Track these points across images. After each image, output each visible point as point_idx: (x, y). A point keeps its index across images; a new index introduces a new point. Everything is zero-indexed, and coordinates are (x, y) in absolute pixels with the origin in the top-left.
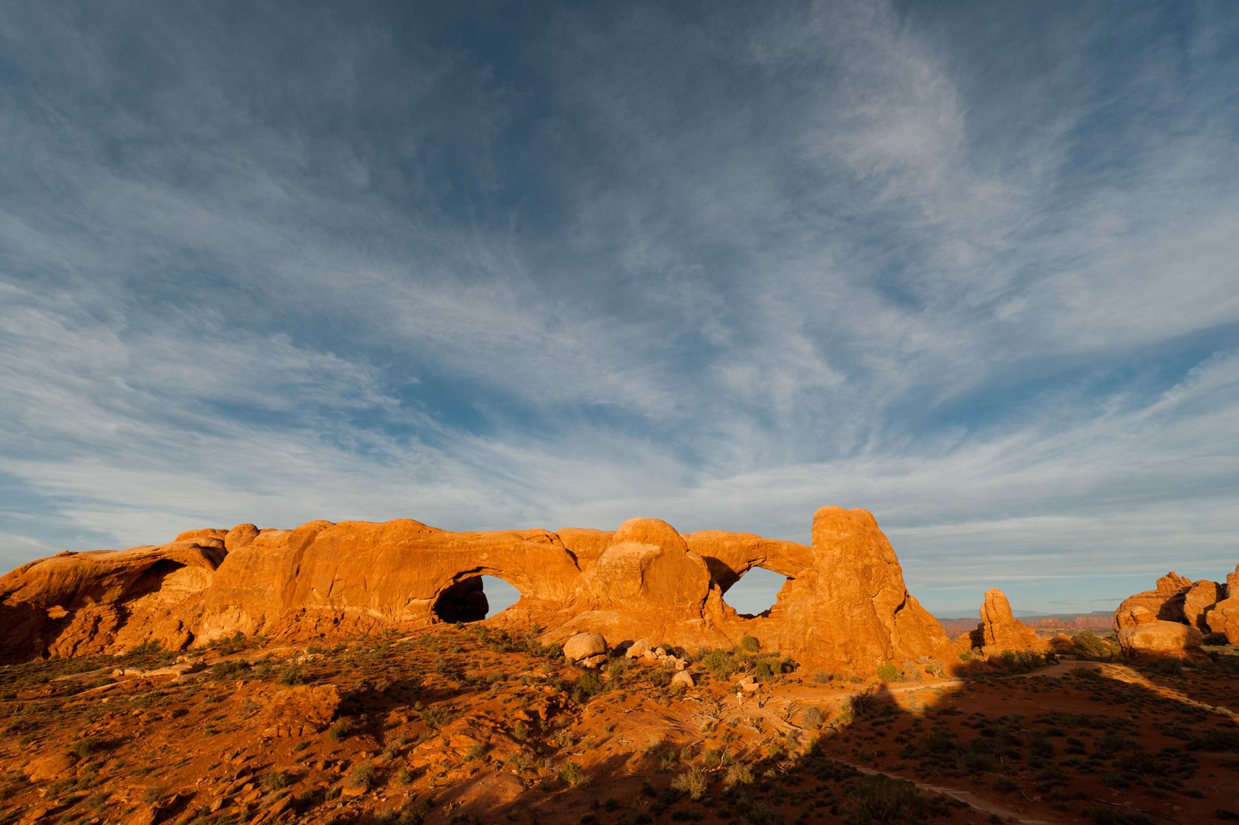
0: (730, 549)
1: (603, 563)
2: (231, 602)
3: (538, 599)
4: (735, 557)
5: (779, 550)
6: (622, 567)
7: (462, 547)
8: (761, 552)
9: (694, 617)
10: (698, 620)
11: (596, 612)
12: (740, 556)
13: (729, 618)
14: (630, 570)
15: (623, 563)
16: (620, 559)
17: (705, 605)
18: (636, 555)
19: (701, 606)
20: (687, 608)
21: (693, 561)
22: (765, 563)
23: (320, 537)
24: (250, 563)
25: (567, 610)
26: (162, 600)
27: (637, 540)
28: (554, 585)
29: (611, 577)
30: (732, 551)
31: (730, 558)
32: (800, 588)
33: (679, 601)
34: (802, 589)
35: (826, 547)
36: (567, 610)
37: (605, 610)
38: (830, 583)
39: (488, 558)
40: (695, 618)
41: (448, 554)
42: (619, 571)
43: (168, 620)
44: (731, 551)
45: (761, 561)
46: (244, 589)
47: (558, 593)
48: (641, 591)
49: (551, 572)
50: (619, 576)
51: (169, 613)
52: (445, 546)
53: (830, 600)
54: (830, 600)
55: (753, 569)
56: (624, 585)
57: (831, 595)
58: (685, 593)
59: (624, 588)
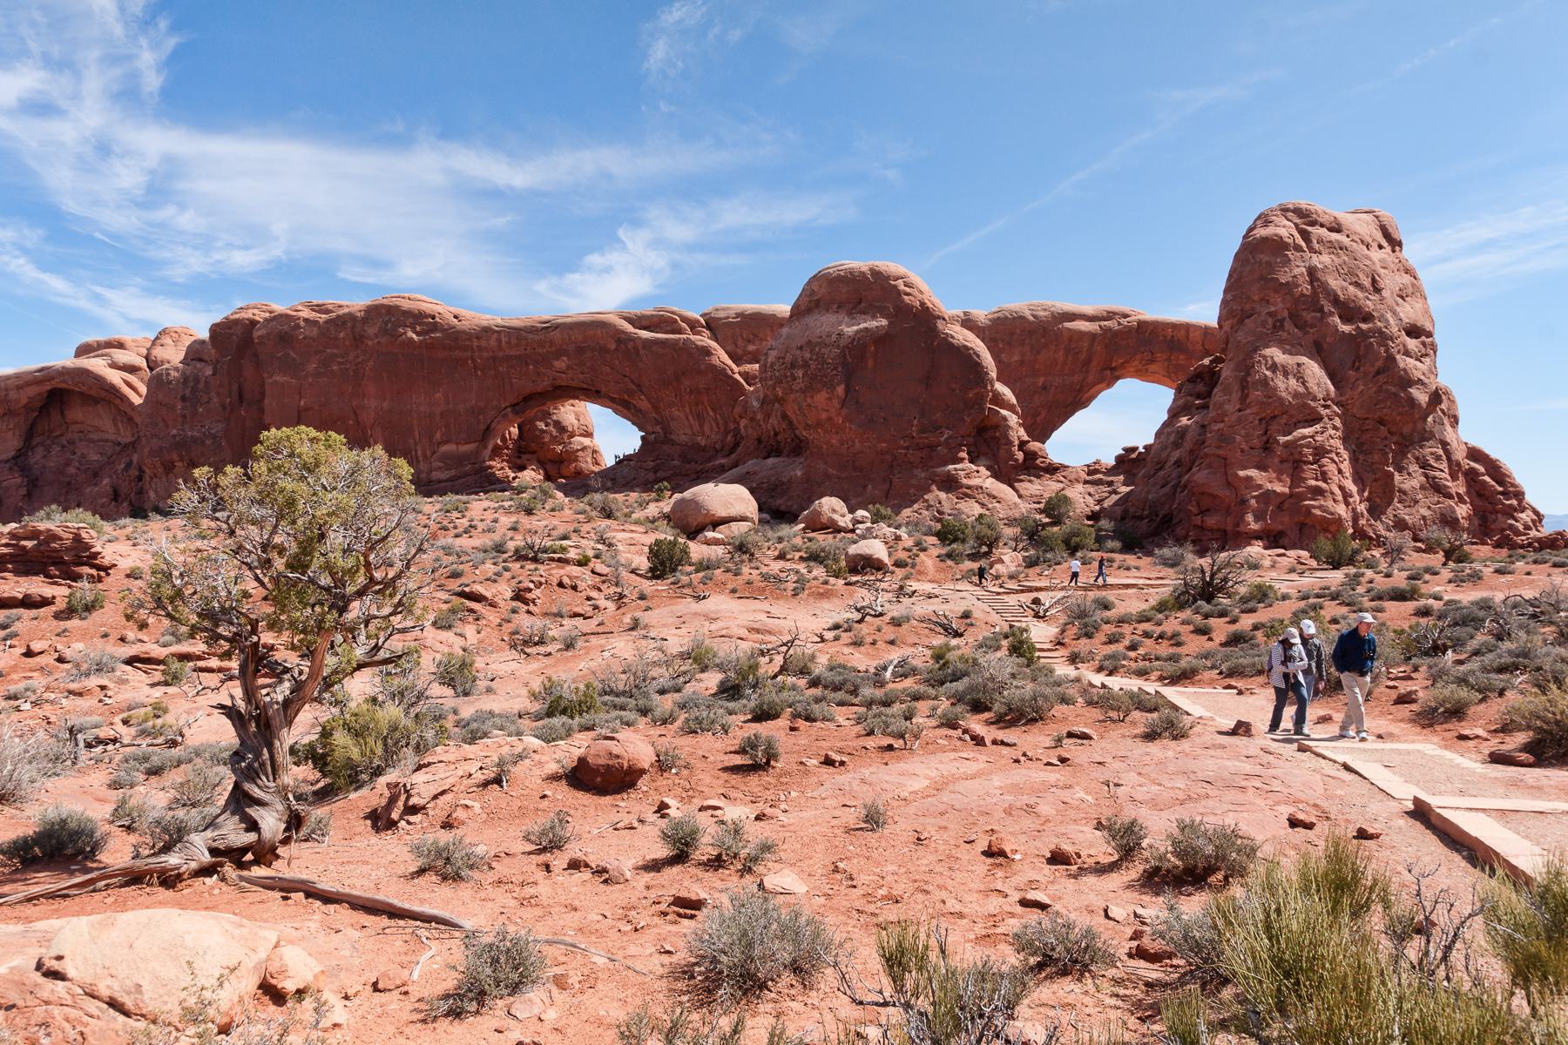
1: (769, 360)
2: (175, 457)
3: (673, 443)
6: (806, 365)
7: (517, 345)
11: (771, 461)
14: (820, 370)
15: (808, 355)
16: (801, 348)
18: (834, 337)
23: (260, 333)
24: (188, 392)
25: (723, 461)
26: (83, 456)
27: (839, 307)
28: (698, 415)
29: (785, 385)
33: (923, 430)
35: (1256, 298)
36: (723, 461)
37: (788, 456)
39: (569, 367)
41: (494, 358)
42: (800, 373)
43: (96, 485)
46: (189, 434)
47: (707, 431)
48: (844, 411)
49: (691, 392)
50: (799, 384)
51: (96, 475)
52: (483, 343)
53: (1240, 410)
54: (1240, 410)
56: (809, 401)
59: (809, 405)
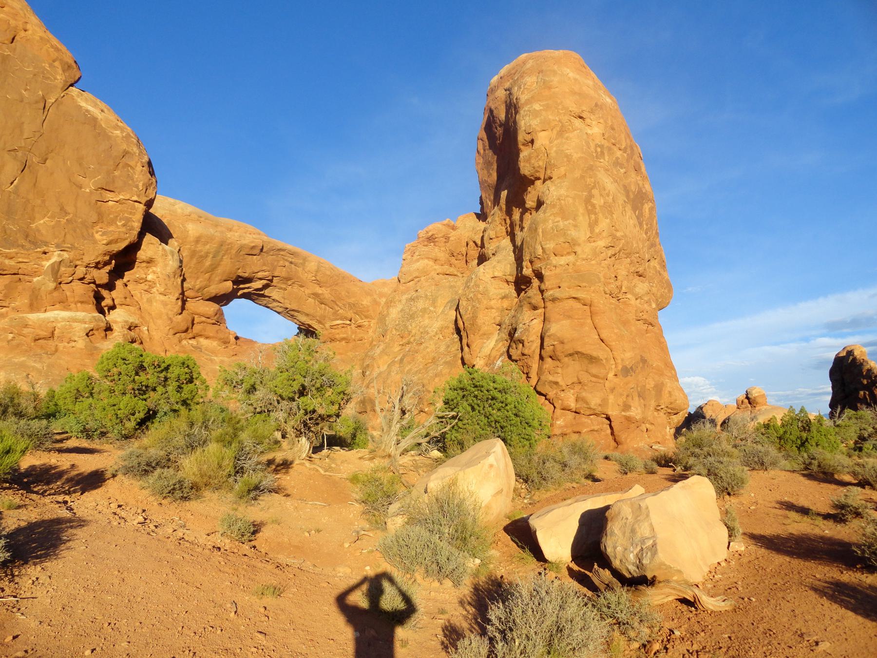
0: (198, 240)
4: (208, 263)
5: (300, 269)
8: (264, 265)
9: (63, 303)
10: (81, 315)
12: (219, 265)
13: (197, 328)
17: (119, 283)
19: (102, 276)
20: (35, 273)
21: (95, 119)
22: (266, 292)
30: (202, 248)
31: (194, 261)
32: (426, 261)
34: (431, 263)
38: (591, 196)
40: (67, 308)
44: (200, 247)
45: (258, 284)
55: (236, 302)
57: (592, 226)
58: (42, 223)
